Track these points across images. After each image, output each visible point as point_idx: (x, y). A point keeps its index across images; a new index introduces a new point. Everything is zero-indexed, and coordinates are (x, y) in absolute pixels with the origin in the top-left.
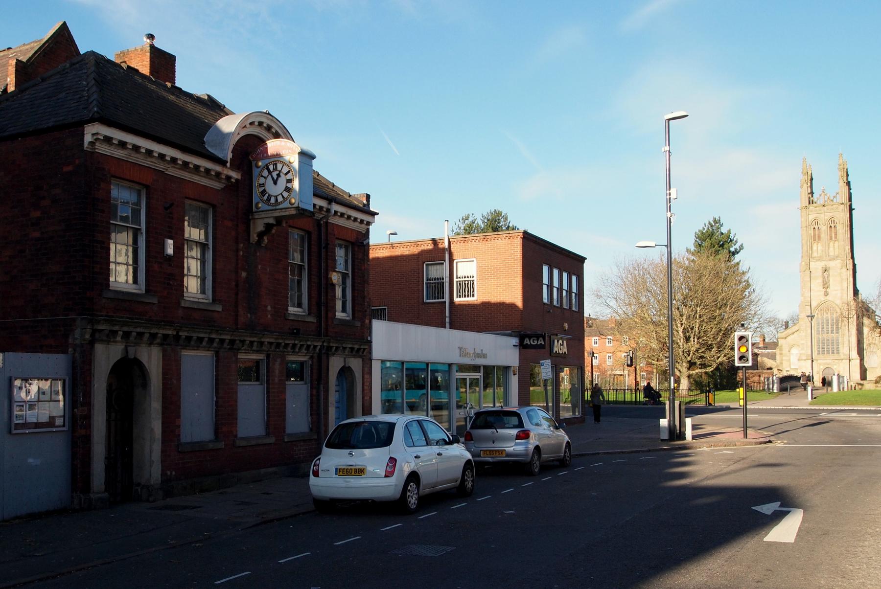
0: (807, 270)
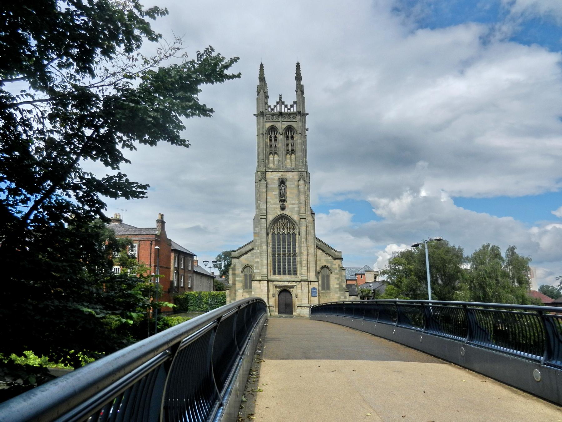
0: (263, 180)
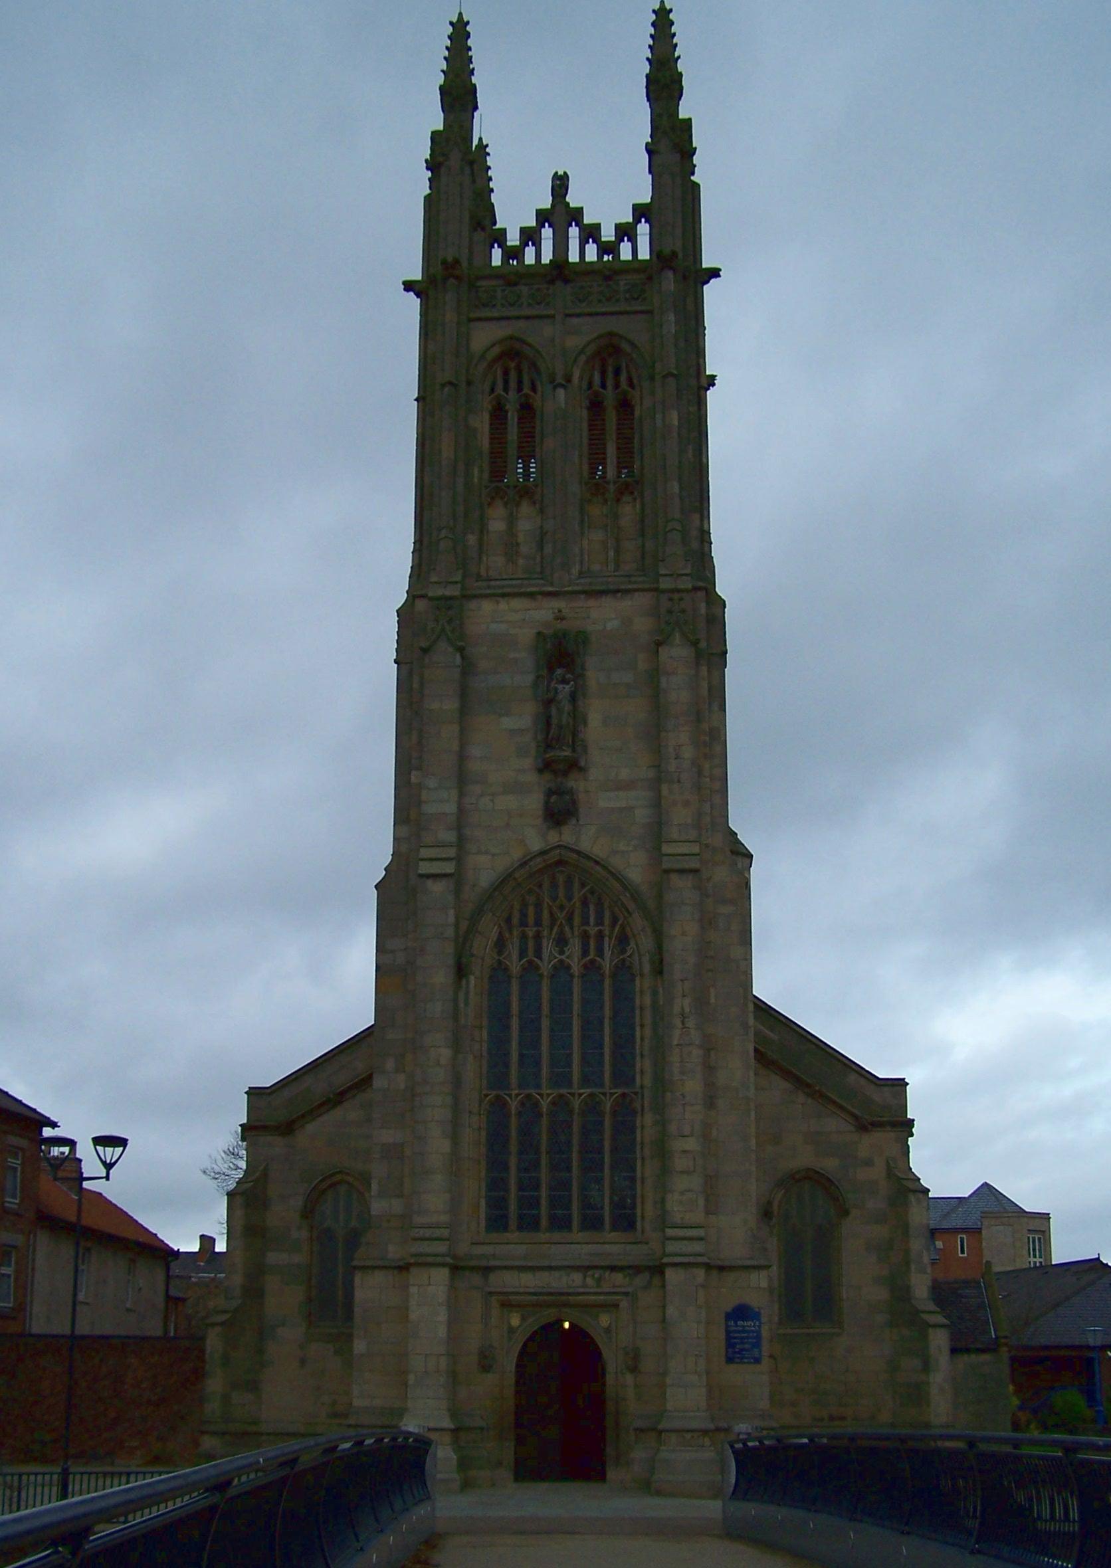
0: (442, 645)
